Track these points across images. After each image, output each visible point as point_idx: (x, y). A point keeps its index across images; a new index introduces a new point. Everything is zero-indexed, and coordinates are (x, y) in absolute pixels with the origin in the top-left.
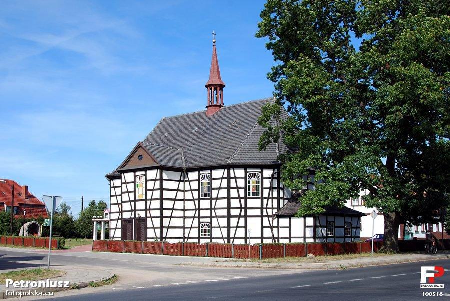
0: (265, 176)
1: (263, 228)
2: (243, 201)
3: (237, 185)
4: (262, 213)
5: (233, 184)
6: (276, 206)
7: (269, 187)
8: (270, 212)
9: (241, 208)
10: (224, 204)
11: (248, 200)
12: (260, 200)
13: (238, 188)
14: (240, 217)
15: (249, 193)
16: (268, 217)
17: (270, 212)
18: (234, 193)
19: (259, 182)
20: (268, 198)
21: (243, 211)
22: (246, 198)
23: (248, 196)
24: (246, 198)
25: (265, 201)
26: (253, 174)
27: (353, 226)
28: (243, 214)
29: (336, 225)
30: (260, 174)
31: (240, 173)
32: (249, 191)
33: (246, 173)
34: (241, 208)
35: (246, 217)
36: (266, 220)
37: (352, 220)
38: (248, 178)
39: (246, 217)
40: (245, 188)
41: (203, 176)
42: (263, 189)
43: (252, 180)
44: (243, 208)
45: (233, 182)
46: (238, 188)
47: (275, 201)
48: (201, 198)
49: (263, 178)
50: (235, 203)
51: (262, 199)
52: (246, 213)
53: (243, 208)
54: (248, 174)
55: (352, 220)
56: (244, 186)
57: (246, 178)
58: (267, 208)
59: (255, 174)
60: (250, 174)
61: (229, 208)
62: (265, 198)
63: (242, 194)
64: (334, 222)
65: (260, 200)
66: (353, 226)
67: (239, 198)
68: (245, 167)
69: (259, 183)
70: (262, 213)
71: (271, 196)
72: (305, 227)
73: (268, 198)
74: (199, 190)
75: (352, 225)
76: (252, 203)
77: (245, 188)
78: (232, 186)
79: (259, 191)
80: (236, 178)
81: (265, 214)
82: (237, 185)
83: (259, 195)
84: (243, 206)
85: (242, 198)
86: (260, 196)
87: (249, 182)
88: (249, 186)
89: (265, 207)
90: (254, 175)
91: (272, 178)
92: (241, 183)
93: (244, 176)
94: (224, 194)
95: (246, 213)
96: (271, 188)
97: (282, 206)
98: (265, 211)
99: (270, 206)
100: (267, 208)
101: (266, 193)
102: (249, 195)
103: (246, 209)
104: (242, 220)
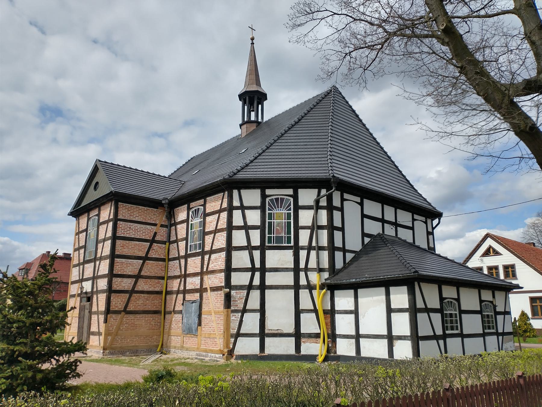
0: (301, 203)
1: (298, 312)
2: (257, 254)
3: (245, 222)
4: (297, 278)
5: (238, 220)
6: (325, 264)
7: (310, 224)
8: (315, 278)
9: (253, 270)
10: (218, 261)
11: (268, 252)
12: (290, 253)
13: (246, 228)
14: (250, 287)
15: (270, 238)
16: (310, 287)
17: (315, 278)
18: (239, 239)
19: (289, 215)
20: (310, 248)
21: (257, 275)
22: (263, 248)
23: (267, 244)
24: (263, 248)
25: (303, 254)
26: (277, 199)
27: (498, 309)
28: (257, 281)
29: (463, 308)
30: (292, 200)
31: (252, 197)
32: (270, 233)
33: (264, 197)
34: (253, 270)
35: (263, 287)
36: (304, 294)
37: (494, 297)
38: (267, 206)
39: (263, 287)
40: (262, 228)
41: (193, 212)
42: (297, 228)
43: (275, 211)
44: (257, 270)
45: (237, 215)
46: (246, 228)
47: (325, 255)
48: (189, 252)
49: (297, 208)
50: (241, 259)
51: (296, 249)
52: (263, 279)
53: (257, 270)
54: (268, 200)
55: (494, 297)
56: (258, 223)
57: (262, 208)
58: (306, 269)
59: (282, 200)
60: (272, 200)
61: (229, 270)
62: (303, 248)
63: (256, 241)
64: (458, 300)
65: (290, 253)
66: (498, 309)
67: (249, 248)
68: (262, 184)
69: (289, 218)
70: (297, 278)
71: (314, 244)
72: (390, 311)
73: (310, 248)
74: (186, 239)
75: (495, 307)
76: (274, 258)
77: (262, 228)
78: (258, 231)
79: (289, 232)
80: (243, 208)
81: (303, 281)
82: (245, 222)
83: (289, 242)
84: (258, 265)
85: (255, 248)
86: (292, 244)
87: (270, 214)
88: (270, 223)
89: (302, 265)
90: (279, 202)
91: (317, 207)
92: (254, 218)
93: (258, 204)
94: (221, 241)
95: (263, 279)
96: (315, 227)
97: (339, 264)
98: (302, 274)
99: (313, 264)
100: (306, 269)
101: (304, 237)
102: (270, 242)
103: (263, 270)
104: (255, 295)
